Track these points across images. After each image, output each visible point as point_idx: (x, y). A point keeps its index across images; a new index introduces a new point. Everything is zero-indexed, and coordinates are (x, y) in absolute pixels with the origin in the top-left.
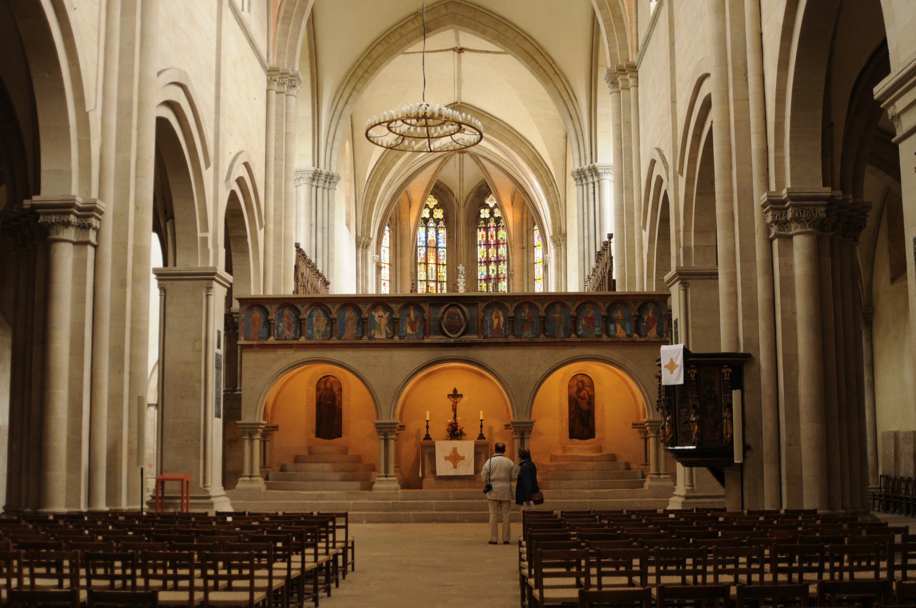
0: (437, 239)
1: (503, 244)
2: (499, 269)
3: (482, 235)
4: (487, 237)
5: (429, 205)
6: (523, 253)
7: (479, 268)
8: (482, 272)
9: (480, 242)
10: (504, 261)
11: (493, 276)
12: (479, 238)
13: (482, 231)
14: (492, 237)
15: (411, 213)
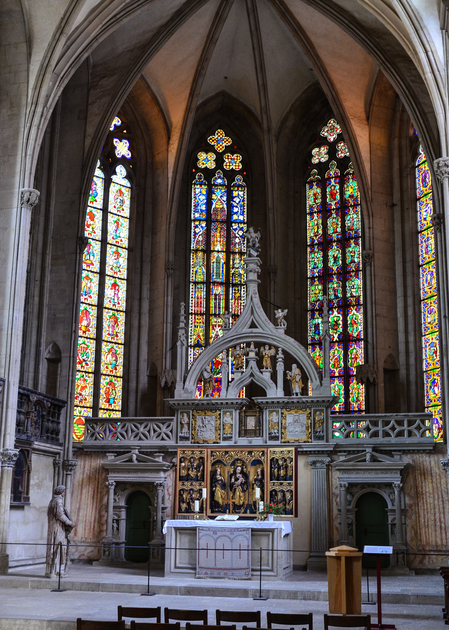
0: (230, 207)
1: (355, 206)
2: (348, 254)
3: (315, 195)
4: (324, 197)
5: (216, 147)
6: (393, 215)
7: (310, 257)
8: (315, 264)
9: (311, 207)
10: (357, 238)
11: (335, 268)
12: (310, 202)
13: (315, 187)
14: (333, 195)
15: (169, 149)
